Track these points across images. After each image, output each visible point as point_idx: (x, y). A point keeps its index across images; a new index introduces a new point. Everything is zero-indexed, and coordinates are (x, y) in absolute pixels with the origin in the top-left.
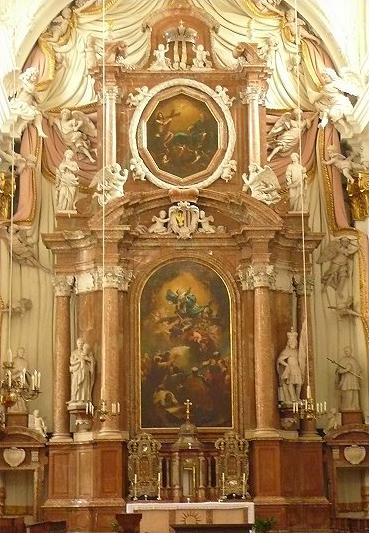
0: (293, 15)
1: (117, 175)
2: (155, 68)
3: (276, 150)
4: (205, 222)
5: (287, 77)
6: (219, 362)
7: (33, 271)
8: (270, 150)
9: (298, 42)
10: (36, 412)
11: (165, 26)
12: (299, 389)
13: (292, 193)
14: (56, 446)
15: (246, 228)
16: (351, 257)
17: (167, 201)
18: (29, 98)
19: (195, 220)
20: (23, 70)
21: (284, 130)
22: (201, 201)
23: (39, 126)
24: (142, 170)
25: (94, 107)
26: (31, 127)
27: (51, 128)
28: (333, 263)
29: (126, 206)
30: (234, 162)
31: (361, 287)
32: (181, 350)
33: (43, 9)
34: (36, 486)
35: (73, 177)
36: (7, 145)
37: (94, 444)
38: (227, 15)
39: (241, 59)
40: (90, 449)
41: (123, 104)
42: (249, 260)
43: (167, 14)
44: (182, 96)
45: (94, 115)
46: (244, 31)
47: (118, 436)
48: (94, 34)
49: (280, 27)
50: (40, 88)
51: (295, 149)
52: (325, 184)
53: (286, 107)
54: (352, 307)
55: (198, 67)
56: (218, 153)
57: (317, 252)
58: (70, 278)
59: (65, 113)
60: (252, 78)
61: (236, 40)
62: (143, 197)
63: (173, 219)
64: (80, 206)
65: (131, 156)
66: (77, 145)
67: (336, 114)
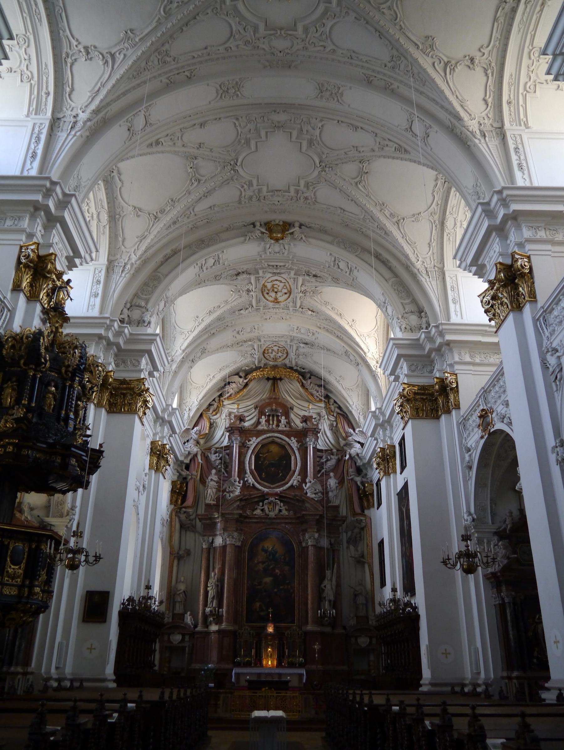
0: (332, 401)
1: (237, 483)
2: (260, 427)
3: (324, 471)
4: (283, 508)
5: (329, 433)
6: (289, 587)
7: (192, 534)
8: (320, 471)
9: (335, 415)
10: (189, 613)
11: (266, 407)
12: (332, 603)
13: (331, 494)
14: (199, 633)
15: (304, 513)
16: (362, 529)
17: (263, 497)
18: (195, 442)
19: (277, 508)
20: (193, 428)
21: (328, 460)
22: (281, 497)
23: (199, 457)
24: (251, 480)
25: (229, 448)
26: (196, 458)
27: (206, 458)
28: (352, 532)
29: (241, 500)
30: (299, 477)
31: (367, 545)
32: (268, 580)
33: (205, 398)
34: (187, 655)
35: (215, 484)
36: (182, 466)
37: (219, 632)
38: (299, 402)
39: (304, 424)
40: (217, 636)
41: (243, 447)
42: (305, 531)
43: (267, 401)
44: (273, 442)
45: (228, 451)
46: (306, 409)
47: (231, 628)
48: (230, 410)
49: (325, 407)
50: (201, 437)
51: (333, 470)
52: (348, 489)
53: (329, 448)
54: (363, 556)
55: (282, 427)
56: (291, 472)
57: (344, 525)
58: (211, 538)
59: (213, 450)
60: (310, 434)
61: (302, 413)
62: (251, 495)
63: (266, 507)
64: (218, 499)
65: (246, 473)
66: (219, 467)
67: (353, 451)
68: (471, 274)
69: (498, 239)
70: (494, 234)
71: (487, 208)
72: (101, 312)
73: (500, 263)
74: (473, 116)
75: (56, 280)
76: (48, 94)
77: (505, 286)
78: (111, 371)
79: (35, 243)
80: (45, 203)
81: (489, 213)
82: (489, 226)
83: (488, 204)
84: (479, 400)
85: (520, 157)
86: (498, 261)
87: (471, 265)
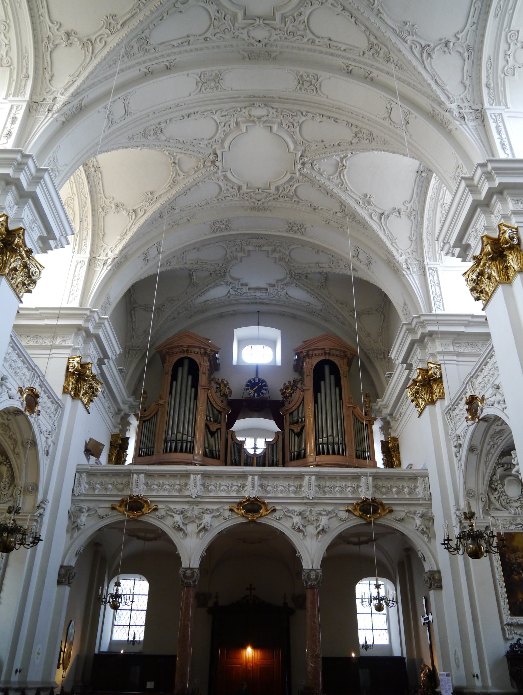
68: (455, 258)
69: (483, 215)
70: (479, 210)
71: (469, 182)
72: (81, 305)
73: (487, 237)
74: (452, 99)
75: (25, 256)
76: (27, 77)
77: (493, 259)
78: (89, 363)
79: (4, 215)
80: (16, 177)
81: (473, 188)
82: (474, 201)
83: (472, 179)
84: (466, 387)
85: (501, 136)
86: (484, 234)
87: (455, 246)
